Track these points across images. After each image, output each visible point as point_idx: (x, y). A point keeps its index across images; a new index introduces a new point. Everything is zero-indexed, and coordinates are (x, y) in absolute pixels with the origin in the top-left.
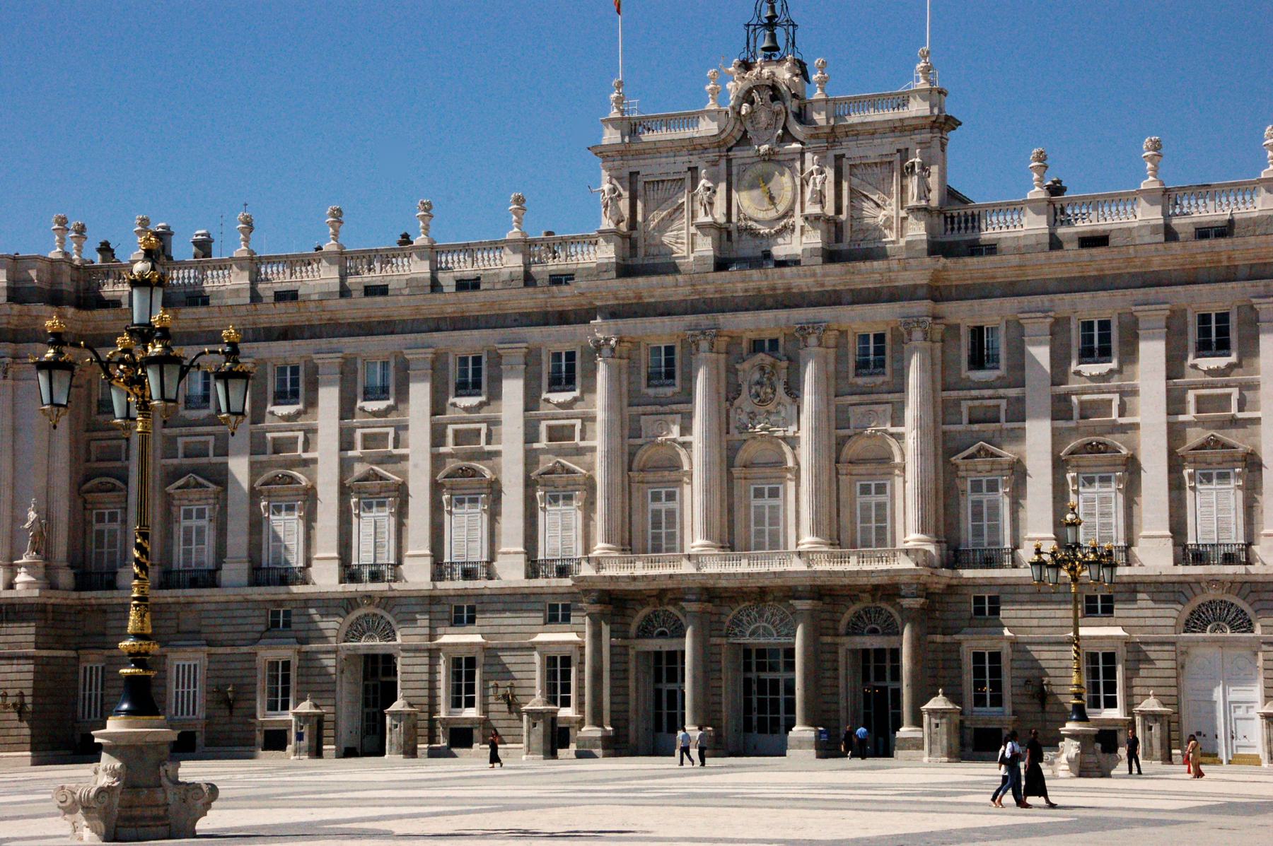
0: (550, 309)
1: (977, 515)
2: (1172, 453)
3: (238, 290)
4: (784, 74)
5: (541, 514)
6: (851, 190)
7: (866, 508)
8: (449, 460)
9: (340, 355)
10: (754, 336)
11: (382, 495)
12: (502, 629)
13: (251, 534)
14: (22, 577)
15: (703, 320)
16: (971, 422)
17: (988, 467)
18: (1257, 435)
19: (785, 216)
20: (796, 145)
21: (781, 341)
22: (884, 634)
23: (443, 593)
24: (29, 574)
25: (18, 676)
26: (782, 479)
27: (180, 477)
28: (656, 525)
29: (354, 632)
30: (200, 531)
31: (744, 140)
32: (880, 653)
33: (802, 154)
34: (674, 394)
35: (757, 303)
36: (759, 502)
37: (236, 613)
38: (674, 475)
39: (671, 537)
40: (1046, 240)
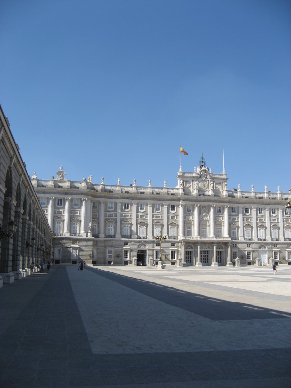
2: (137, 223)
4: (206, 169)
5: (170, 229)
6: (215, 186)
7: (218, 231)
8: (155, 220)
10: (202, 206)
12: (165, 247)
13: (120, 230)
14: (89, 235)
16: (232, 220)
18: (266, 224)
21: (207, 207)
22: (221, 249)
24: (91, 234)
26: (206, 227)
27: (109, 220)
28: (188, 232)
29: (139, 246)
30: (111, 229)
31: (200, 177)
32: (220, 252)
36: (203, 230)
37: (119, 243)
38: (190, 225)
39: (190, 234)
40: (242, 196)
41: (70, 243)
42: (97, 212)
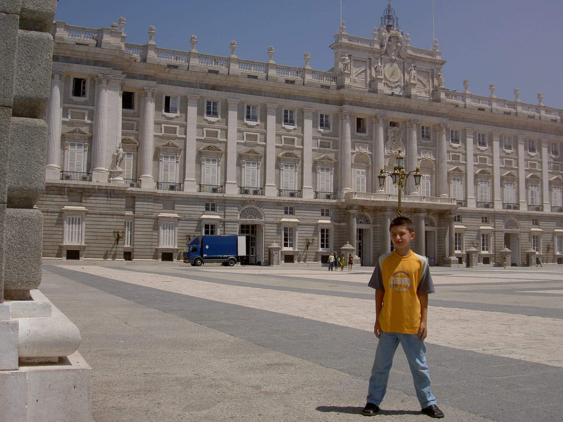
0: (323, 98)
1: (454, 190)
3: (193, 66)
9: (239, 100)
11: (254, 160)
12: (305, 217)
15: (381, 112)
17: (457, 175)
19: (398, 82)
20: (402, 60)
21: (400, 124)
23: (283, 201)
25: (116, 224)
30: (172, 167)
31: (386, 53)
33: (404, 63)
34: (366, 136)
35: (398, 109)
41: (60, 200)
42: (138, 119)
